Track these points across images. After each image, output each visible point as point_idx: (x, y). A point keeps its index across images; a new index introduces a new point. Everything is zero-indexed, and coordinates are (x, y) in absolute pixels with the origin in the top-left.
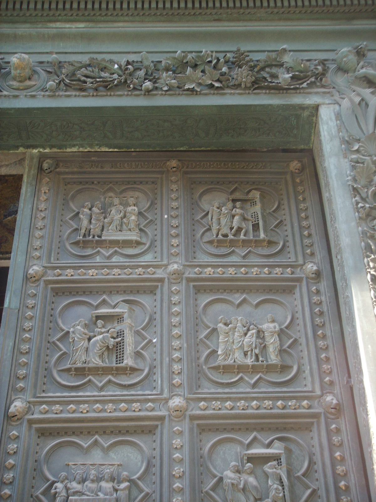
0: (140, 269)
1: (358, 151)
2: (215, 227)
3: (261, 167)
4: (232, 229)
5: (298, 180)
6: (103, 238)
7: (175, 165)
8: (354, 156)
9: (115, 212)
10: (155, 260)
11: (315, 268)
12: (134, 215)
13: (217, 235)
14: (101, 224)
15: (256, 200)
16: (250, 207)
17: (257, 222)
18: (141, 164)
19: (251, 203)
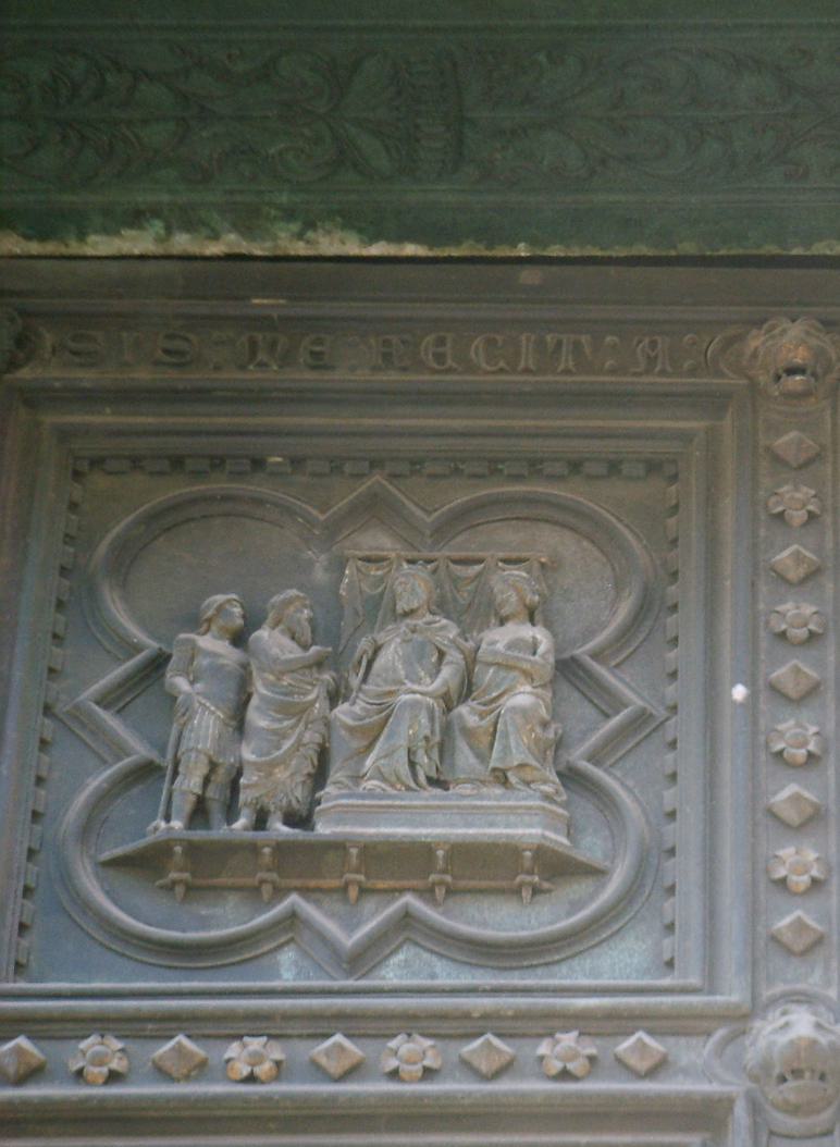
0: (568, 1039)
6: (324, 829)
9: (407, 662)
10: (666, 982)
14: (312, 737)
18: (577, 346)
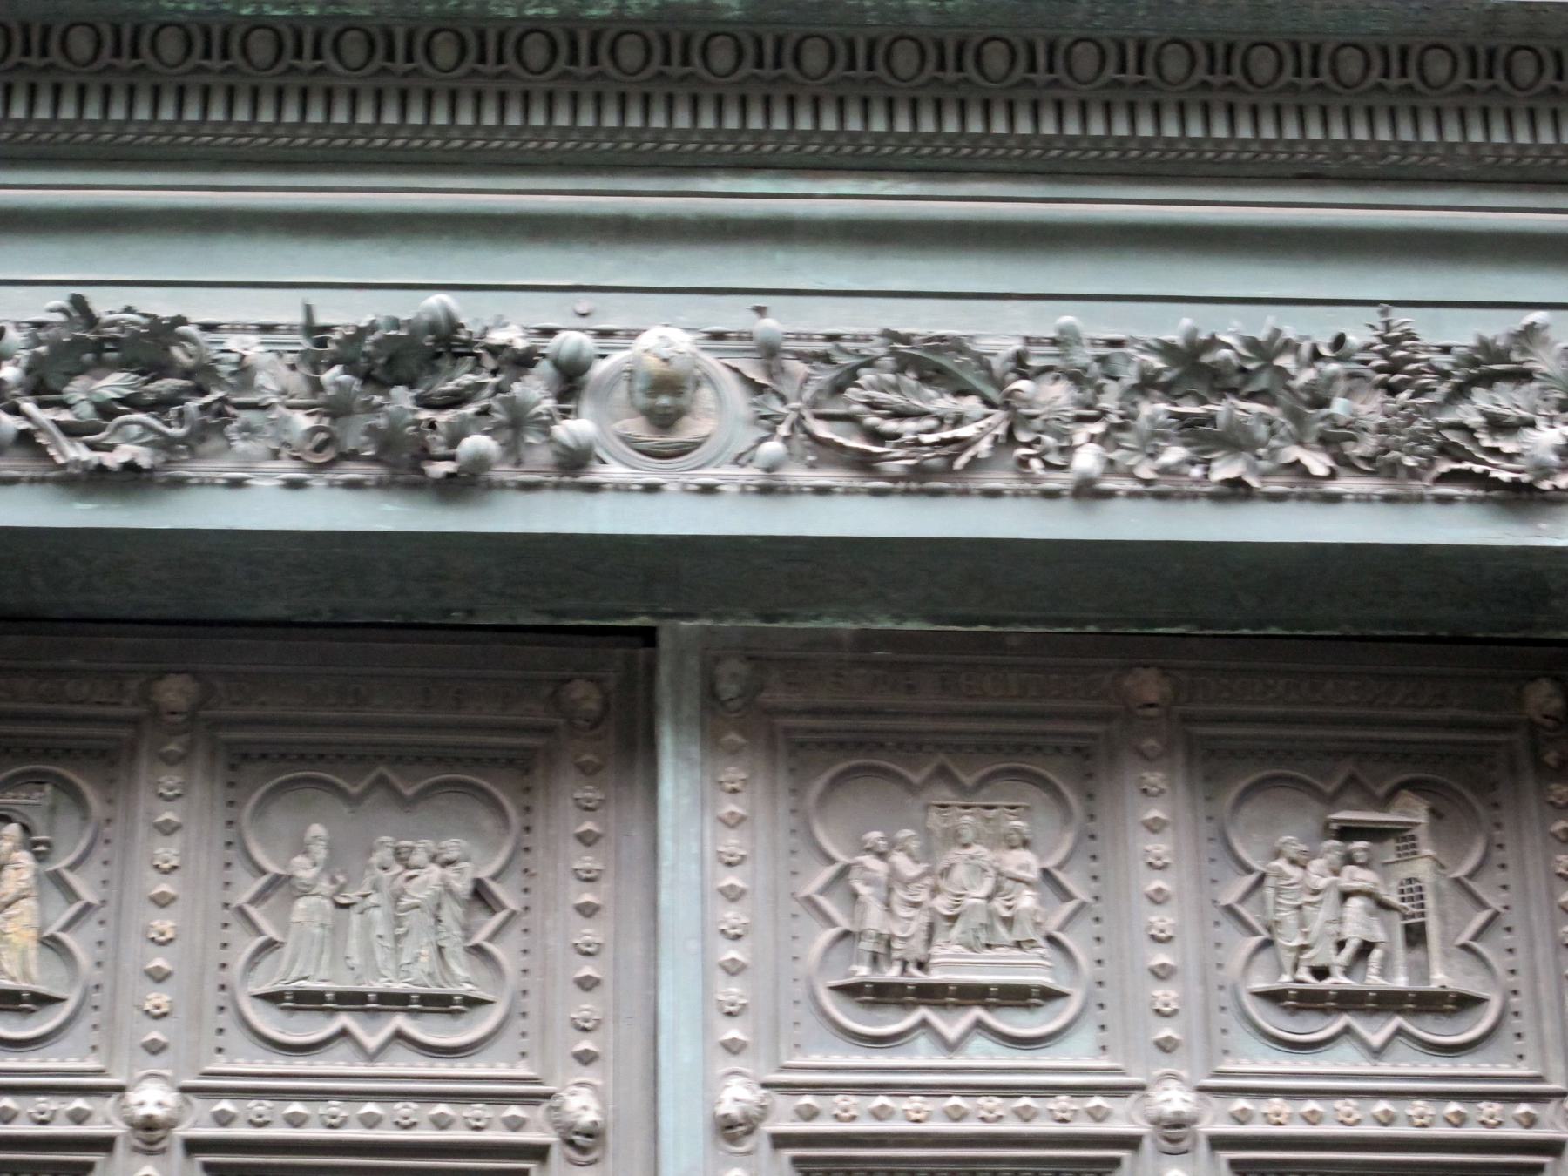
2: (1290, 939)
4: (1341, 945)
5: (1551, 758)
6: (936, 976)
7: (1153, 697)
12: (1028, 883)
13: (1296, 968)
15: (1416, 831)
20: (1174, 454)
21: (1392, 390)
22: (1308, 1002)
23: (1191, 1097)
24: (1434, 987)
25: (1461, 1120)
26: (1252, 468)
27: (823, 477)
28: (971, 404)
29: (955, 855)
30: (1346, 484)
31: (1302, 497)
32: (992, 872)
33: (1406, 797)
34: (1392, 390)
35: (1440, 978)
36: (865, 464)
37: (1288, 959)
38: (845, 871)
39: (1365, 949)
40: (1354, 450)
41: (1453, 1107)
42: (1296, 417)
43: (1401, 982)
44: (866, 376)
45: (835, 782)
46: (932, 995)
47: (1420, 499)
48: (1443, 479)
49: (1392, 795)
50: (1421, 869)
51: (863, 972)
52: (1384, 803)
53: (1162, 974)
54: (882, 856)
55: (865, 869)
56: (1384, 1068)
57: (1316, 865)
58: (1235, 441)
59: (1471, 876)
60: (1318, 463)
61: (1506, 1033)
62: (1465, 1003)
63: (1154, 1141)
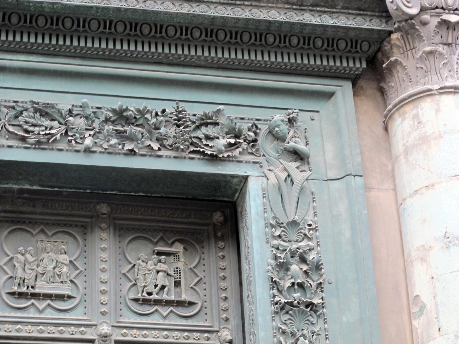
1: (280, 236)
2: (141, 284)
3: (186, 216)
4: (156, 286)
5: (219, 234)
6: (37, 291)
7: (105, 212)
8: (276, 242)
9: (48, 261)
10: (85, 318)
11: (229, 338)
13: (143, 292)
14: (35, 274)
15: (179, 254)
16: (173, 261)
17: (179, 279)
19: (174, 256)
20: (114, 141)
21: (178, 126)
22: (146, 302)
23: (110, 328)
24: (182, 299)
25: (188, 338)
26: (137, 147)
27: (10, 143)
28: (55, 124)
29: (45, 255)
30: (163, 152)
31: (150, 156)
32: (55, 261)
33: (177, 244)
34: (178, 126)
35: (184, 297)
36: (23, 139)
37: (140, 290)
38: (12, 259)
39: (163, 287)
40: (166, 143)
41: (186, 334)
42: (150, 132)
43: (173, 298)
44: (25, 113)
45: (10, 232)
46: (35, 296)
47: (185, 158)
48: (191, 152)
49: (173, 243)
50: (180, 265)
51: (15, 289)
52: (172, 245)
53: (103, 292)
54: (23, 255)
55: (18, 258)
56: (167, 322)
57: (150, 262)
58: (131, 139)
59: (194, 267)
60: (156, 146)
61: (202, 313)
62: (191, 304)
63: (99, 341)
